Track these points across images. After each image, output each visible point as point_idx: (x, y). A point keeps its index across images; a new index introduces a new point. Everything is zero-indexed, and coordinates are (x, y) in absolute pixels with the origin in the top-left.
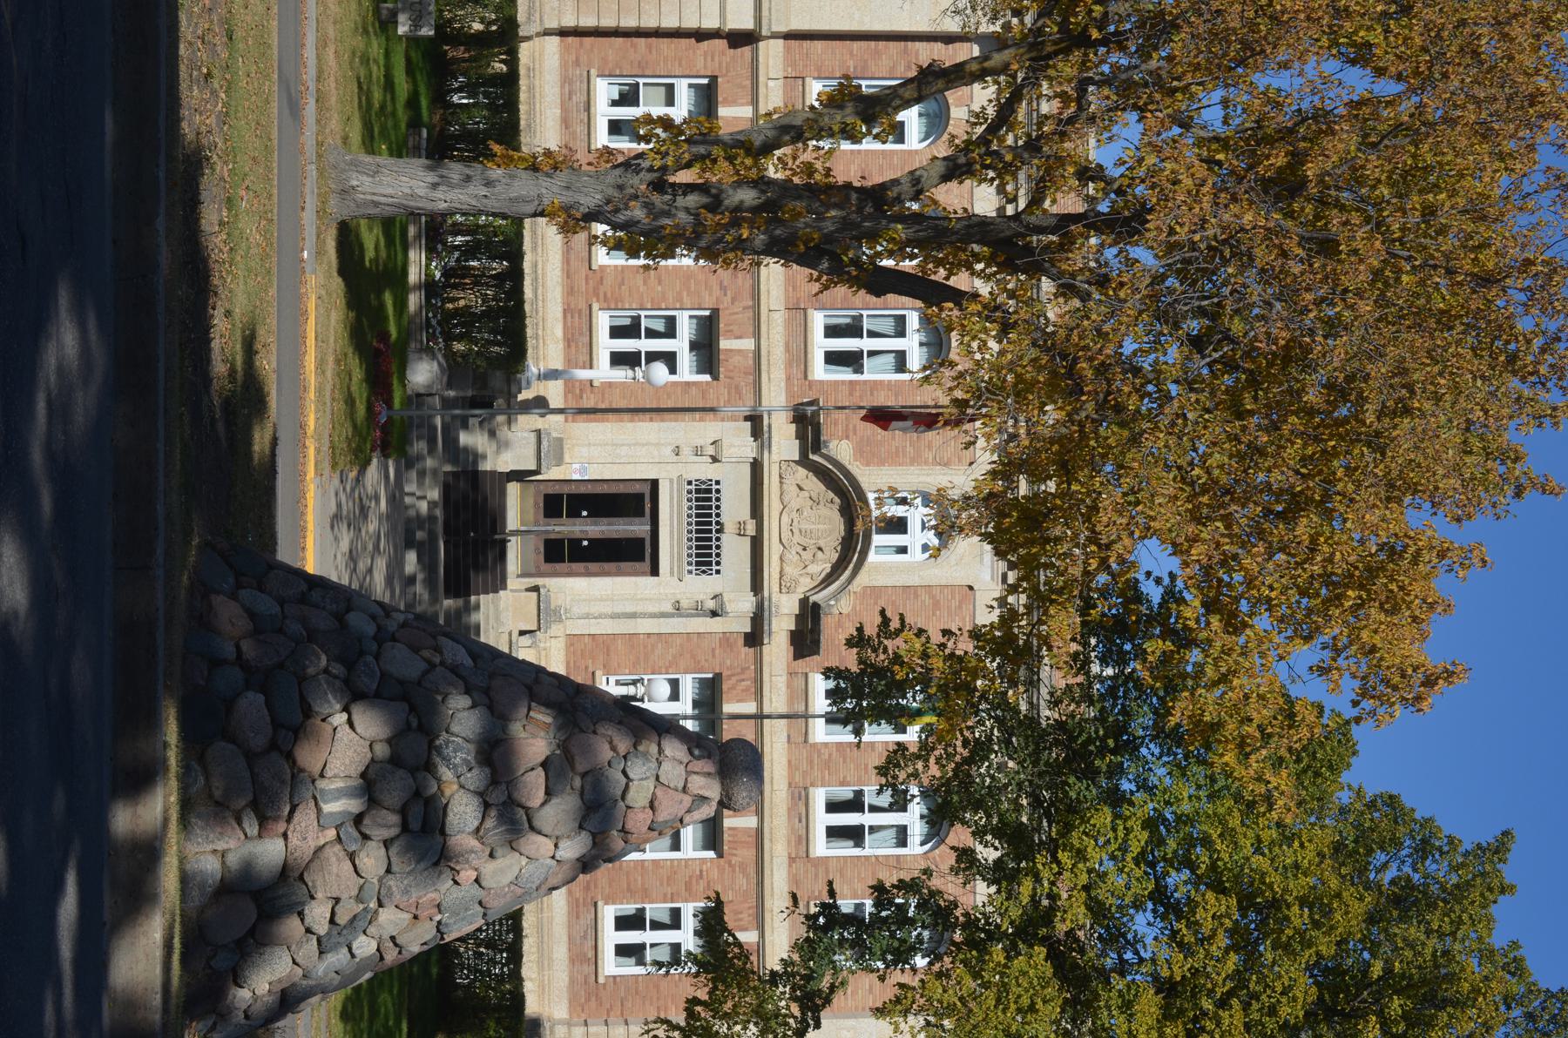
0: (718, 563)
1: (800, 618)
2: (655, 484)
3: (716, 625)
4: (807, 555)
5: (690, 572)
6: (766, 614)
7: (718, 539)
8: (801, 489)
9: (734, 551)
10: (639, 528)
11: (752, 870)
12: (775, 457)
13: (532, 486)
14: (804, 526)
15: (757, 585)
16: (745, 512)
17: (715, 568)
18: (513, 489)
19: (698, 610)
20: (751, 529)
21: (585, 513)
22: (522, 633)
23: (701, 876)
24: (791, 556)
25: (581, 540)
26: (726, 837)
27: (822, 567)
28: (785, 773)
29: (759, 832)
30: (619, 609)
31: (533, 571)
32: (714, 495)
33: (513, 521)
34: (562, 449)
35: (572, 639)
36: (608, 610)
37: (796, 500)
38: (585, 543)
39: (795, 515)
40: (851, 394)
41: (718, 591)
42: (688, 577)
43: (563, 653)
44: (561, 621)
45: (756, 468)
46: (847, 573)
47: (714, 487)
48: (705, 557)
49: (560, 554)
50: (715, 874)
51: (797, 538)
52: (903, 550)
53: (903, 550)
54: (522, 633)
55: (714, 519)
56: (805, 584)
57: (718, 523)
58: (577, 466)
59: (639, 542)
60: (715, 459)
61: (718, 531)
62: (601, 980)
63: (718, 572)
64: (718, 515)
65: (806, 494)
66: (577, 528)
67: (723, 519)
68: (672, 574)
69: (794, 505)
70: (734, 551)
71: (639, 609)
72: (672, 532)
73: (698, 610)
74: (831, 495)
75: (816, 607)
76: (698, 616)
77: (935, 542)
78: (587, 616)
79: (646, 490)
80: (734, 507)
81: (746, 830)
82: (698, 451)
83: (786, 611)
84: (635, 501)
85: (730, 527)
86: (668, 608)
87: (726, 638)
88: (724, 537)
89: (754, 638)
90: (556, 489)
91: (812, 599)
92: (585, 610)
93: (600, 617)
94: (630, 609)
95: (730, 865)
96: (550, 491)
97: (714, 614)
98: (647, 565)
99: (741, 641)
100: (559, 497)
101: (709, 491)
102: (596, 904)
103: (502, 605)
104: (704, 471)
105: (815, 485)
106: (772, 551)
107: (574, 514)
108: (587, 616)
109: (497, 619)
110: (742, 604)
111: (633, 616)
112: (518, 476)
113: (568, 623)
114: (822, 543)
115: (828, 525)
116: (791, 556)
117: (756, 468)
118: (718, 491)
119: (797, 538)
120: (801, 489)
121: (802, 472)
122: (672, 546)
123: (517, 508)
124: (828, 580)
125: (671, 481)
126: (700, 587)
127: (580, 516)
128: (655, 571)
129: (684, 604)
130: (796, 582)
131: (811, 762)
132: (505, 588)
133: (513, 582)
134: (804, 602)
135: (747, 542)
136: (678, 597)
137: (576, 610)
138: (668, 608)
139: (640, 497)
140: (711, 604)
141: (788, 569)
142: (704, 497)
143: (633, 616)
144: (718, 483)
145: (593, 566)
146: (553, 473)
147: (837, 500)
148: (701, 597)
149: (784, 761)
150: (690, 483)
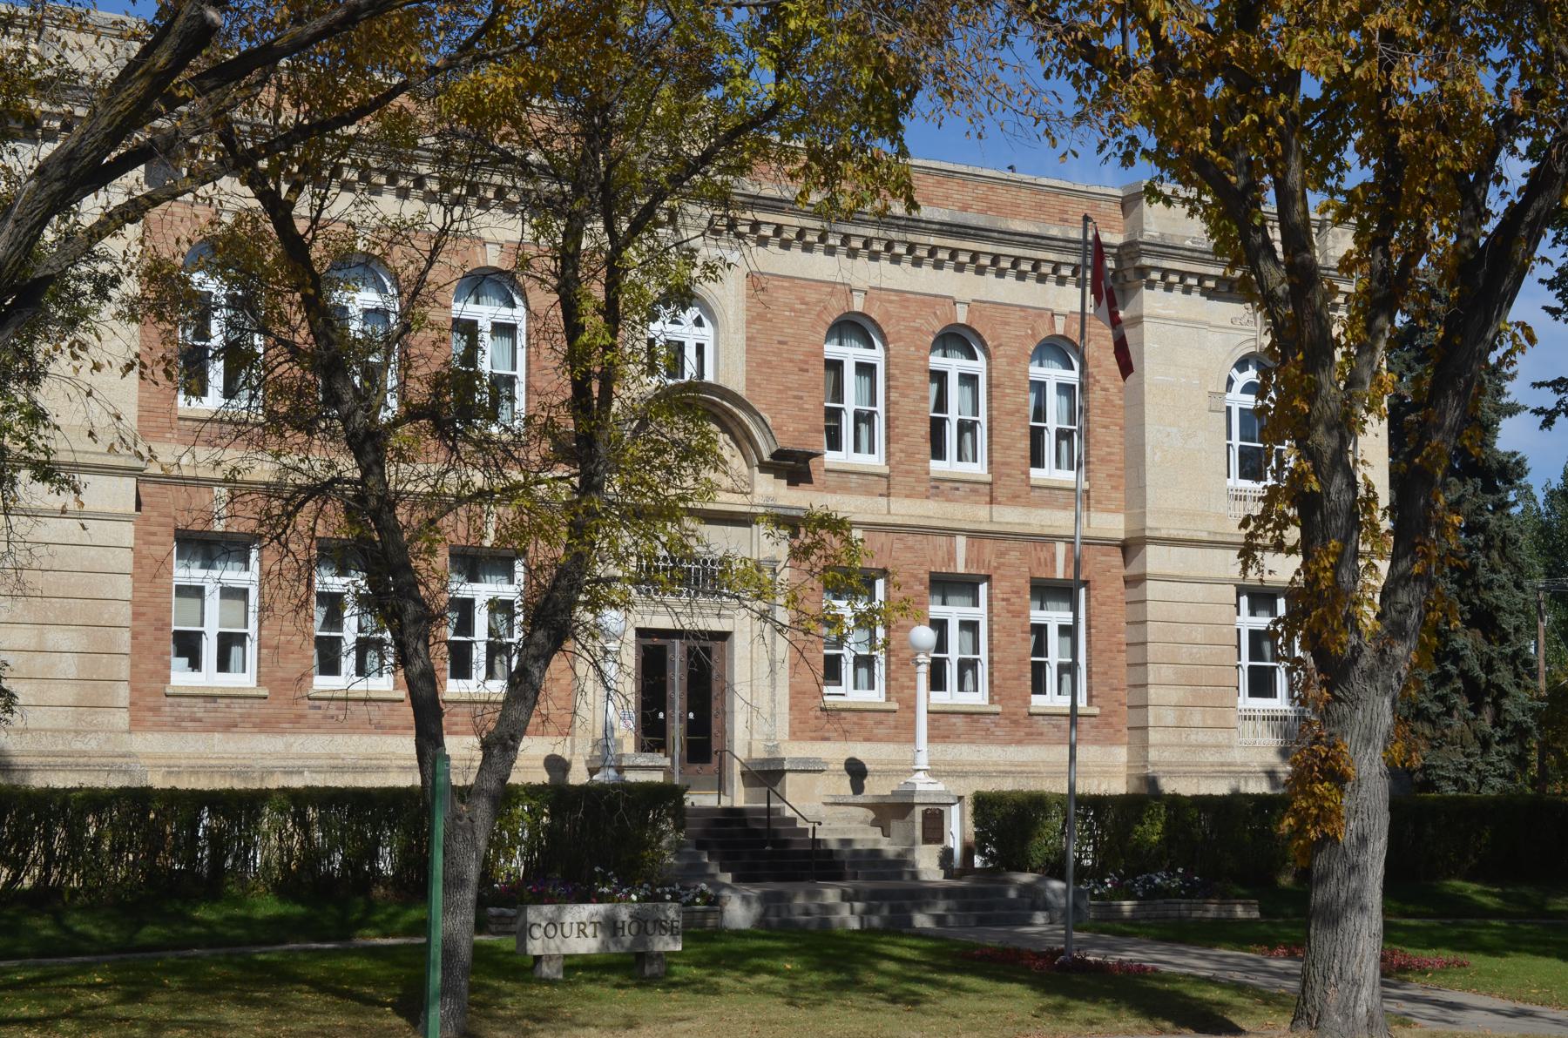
10: (677, 653)
11: (1004, 545)
21: (661, 715)
23: (1007, 600)
25: (689, 721)
26: (973, 571)
28: (918, 502)
29: (974, 535)
35: (794, 735)
36: (768, 690)
38: (691, 715)
50: (1005, 585)
52: (700, 349)
53: (700, 349)
59: (690, 652)
62: (264, 692)
77: (693, 312)
81: (969, 549)
91: (766, 458)
95: (997, 568)
102: (1031, 714)
111: (772, 663)
124: (743, 439)
127: (664, 721)
128: (724, 636)
131: (908, 472)
134: (764, 467)
149: (907, 502)
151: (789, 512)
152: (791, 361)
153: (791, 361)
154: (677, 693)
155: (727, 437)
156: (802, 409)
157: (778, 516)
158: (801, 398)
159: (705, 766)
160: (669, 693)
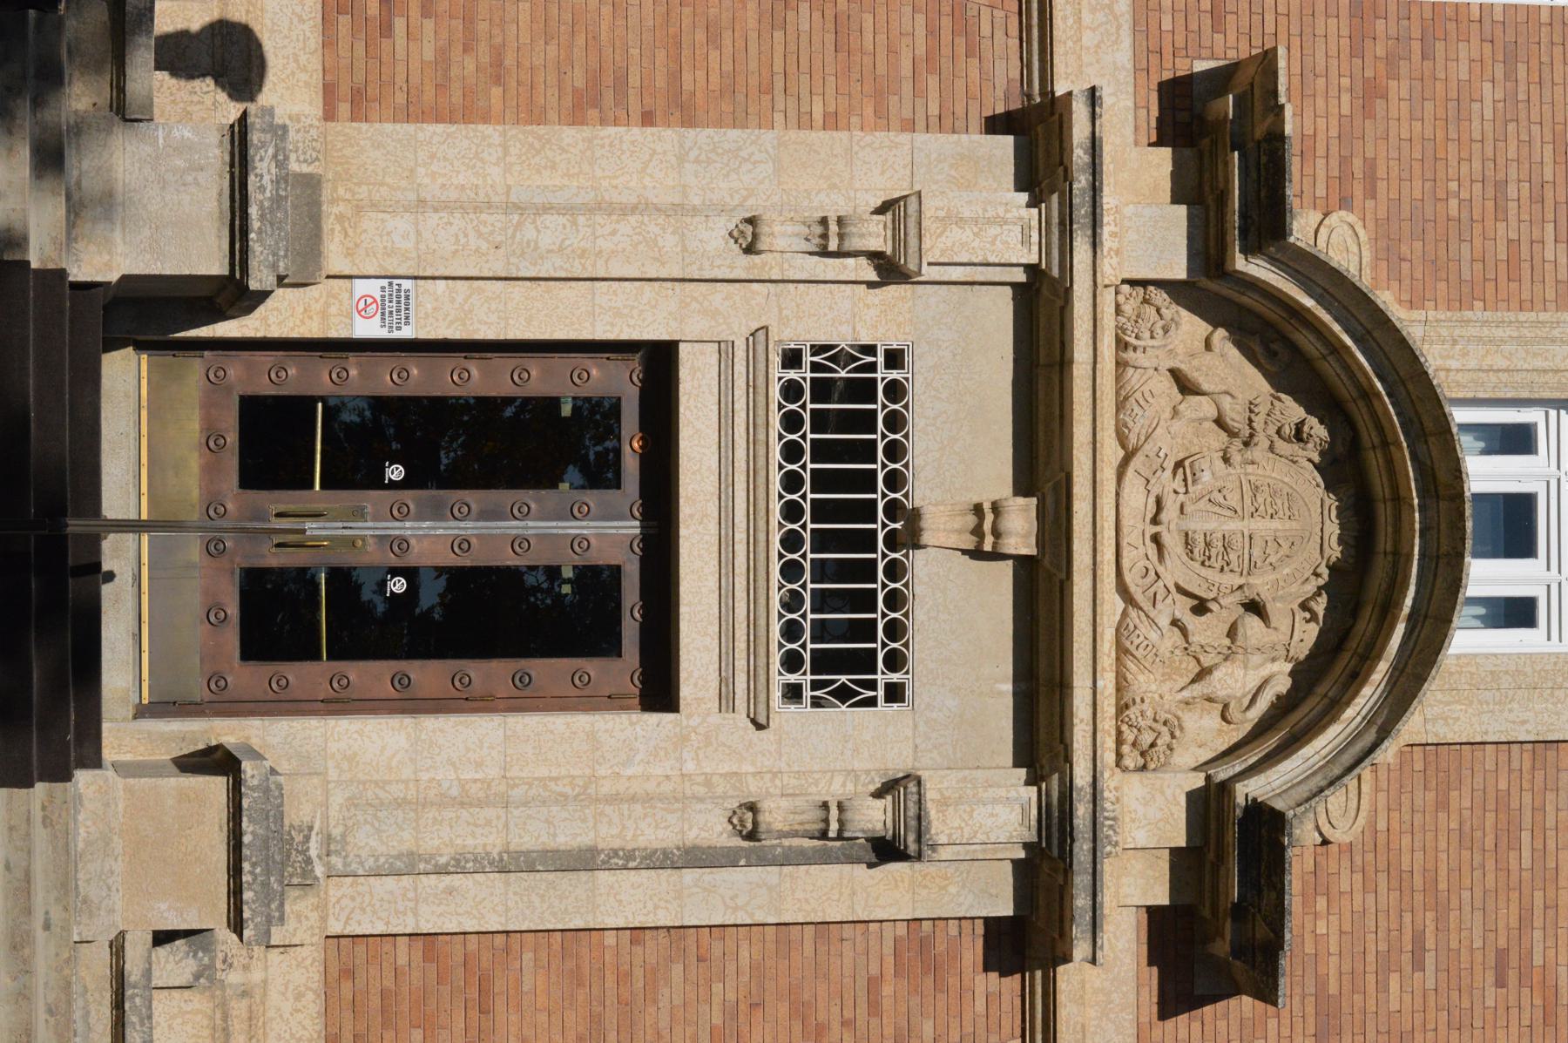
0: (895, 661)
1: (1187, 864)
2: (659, 363)
3: (890, 893)
4: (1208, 631)
5: (793, 693)
6: (1082, 849)
7: (894, 571)
8: (1186, 386)
9: (956, 616)
10: (605, 531)
12: (1111, 270)
13: (195, 368)
14: (1203, 523)
15: (1040, 737)
16: (989, 466)
17: (882, 677)
18: (124, 375)
19: (829, 837)
20: (1020, 529)
21: (395, 472)
22: (162, 938)
24: (1155, 636)
27: (1261, 671)
30: (531, 836)
31: (198, 690)
32: (881, 406)
33: (121, 487)
34: (315, 218)
35: (349, 953)
36: (491, 841)
37: (1177, 431)
39: (1167, 483)
40: (1357, 51)
41: (898, 764)
42: (785, 715)
43: (312, 1005)
44: (308, 884)
45: (1040, 304)
46: (1369, 695)
47: (883, 375)
48: (846, 642)
49: (297, 625)
51: (1177, 569)
54: (162, 938)
55: (880, 496)
56: (1205, 735)
57: (893, 510)
58: (373, 288)
59: (598, 582)
60: (890, 270)
61: (892, 541)
63: (895, 693)
64: (894, 480)
65: (1205, 407)
66: (366, 529)
67: (921, 492)
68: (726, 700)
69: (1168, 441)
70: (956, 616)
71: (607, 834)
72: (725, 545)
73: (829, 837)
74: (1292, 411)
75: (1266, 826)
76: (825, 858)
78: (408, 866)
79: (620, 382)
80: (954, 450)
82: (828, 240)
83: (1141, 837)
84: (582, 423)
85: (943, 526)
86: (714, 830)
87: (919, 940)
88: (921, 565)
89: (1029, 938)
90: (294, 378)
91: (1247, 790)
92: (404, 840)
93: (457, 866)
94: (570, 835)
96: (264, 387)
97: (886, 850)
98: (628, 663)
99: (973, 950)
100: (296, 409)
101: (864, 390)
103: (85, 828)
104: (850, 315)
105: (1233, 375)
106: (1093, 611)
107: (354, 468)
108: (408, 866)
109: (66, 885)
110: (988, 812)
111: (584, 861)
112: (156, 313)
113: (336, 891)
114: (1261, 585)
115: (1285, 523)
116: (1155, 636)
117: (1040, 304)
118: (895, 391)
119: (1177, 569)
120: (1186, 386)
121: (1191, 326)
122: (725, 596)
123: (143, 434)
124: (1288, 721)
125: (725, 349)
126: (831, 753)
127: (376, 481)
128: (659, 691)
129: (775, 815)
130: (1174, 728)
132: (94, 760)
133: (122, 736)
134: (1208, 804)
135: (1000, 579)
136: (753, 789)
137: (367, 843)
138: (714, 830)
139: (599, 415)
140: (874, 816)
141: (1144, 683)
142: (843, 417)
143: (584, 861)
144: (895, 359)
145: (428, 674)
146: (281, 316)
147: (1318, 430)
148: (836, 789)
150: (792, 359)
151: (1081, 881)
152: (1525, 921)
153: (1525, 921)
154: (469, 528)
155: (1283, 685)
156: (1385, 966)
157: (1066, 856)
158: (1419, 965)
159: (231, 639)
160: (474, 498)
